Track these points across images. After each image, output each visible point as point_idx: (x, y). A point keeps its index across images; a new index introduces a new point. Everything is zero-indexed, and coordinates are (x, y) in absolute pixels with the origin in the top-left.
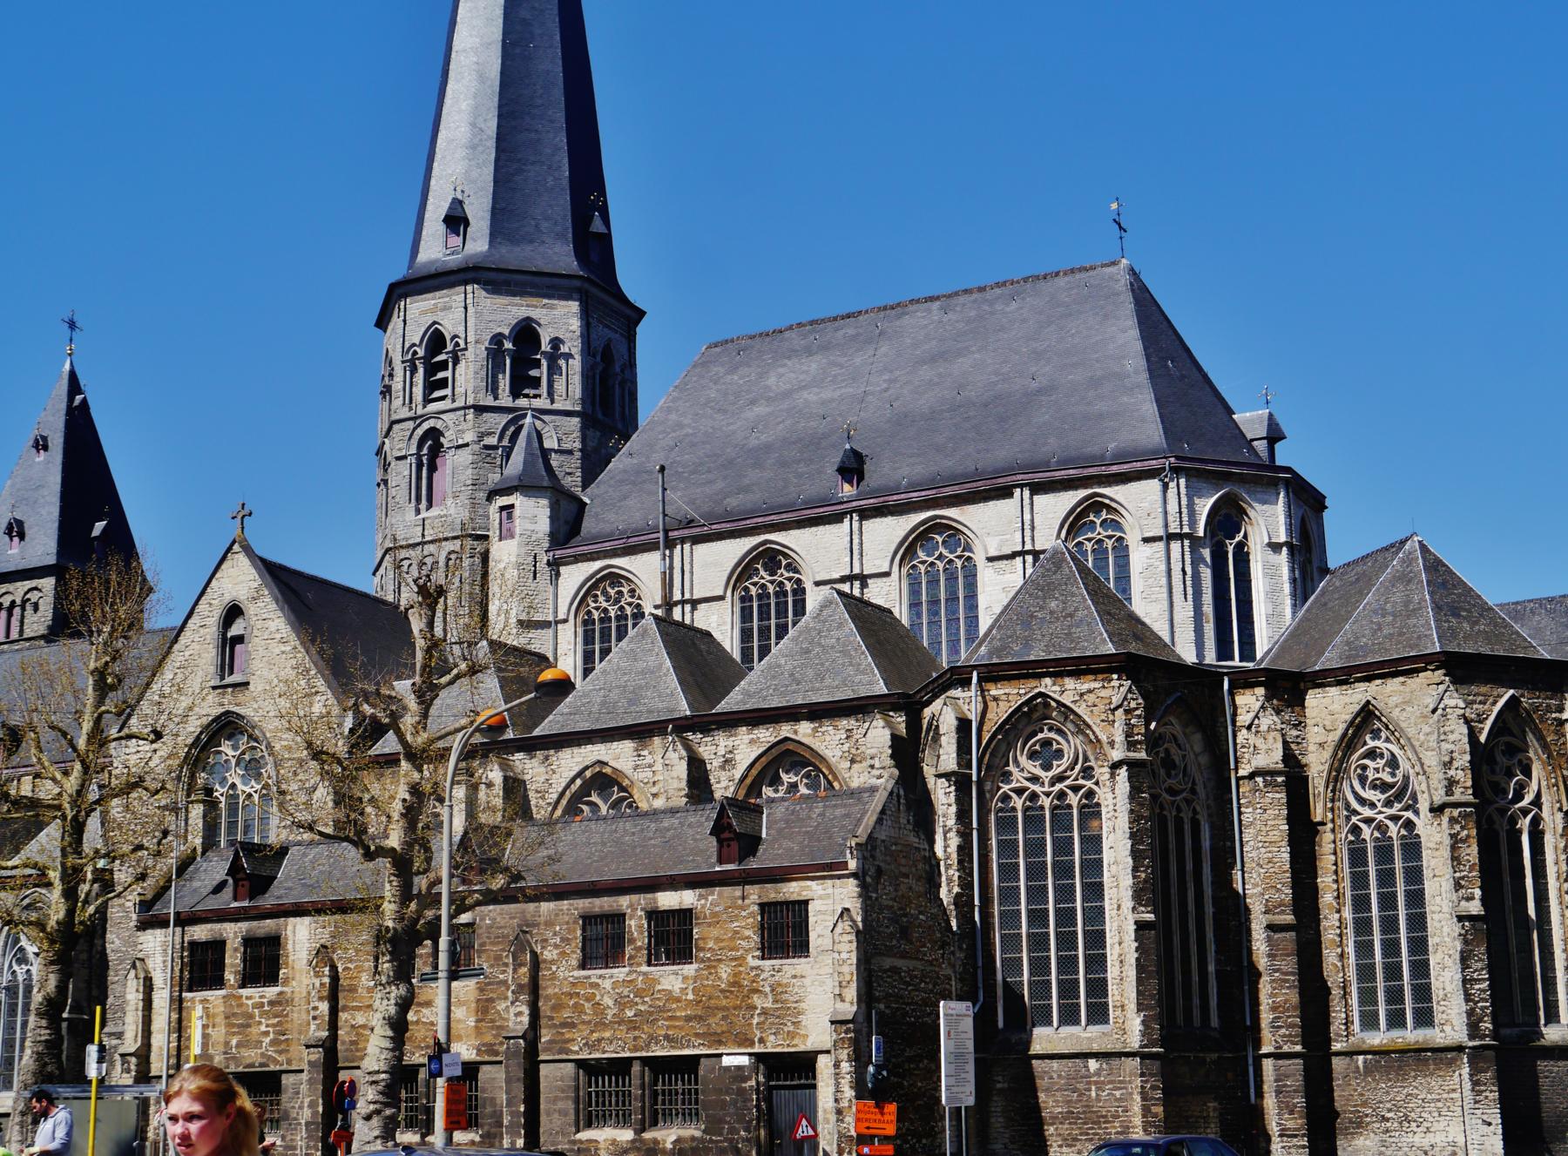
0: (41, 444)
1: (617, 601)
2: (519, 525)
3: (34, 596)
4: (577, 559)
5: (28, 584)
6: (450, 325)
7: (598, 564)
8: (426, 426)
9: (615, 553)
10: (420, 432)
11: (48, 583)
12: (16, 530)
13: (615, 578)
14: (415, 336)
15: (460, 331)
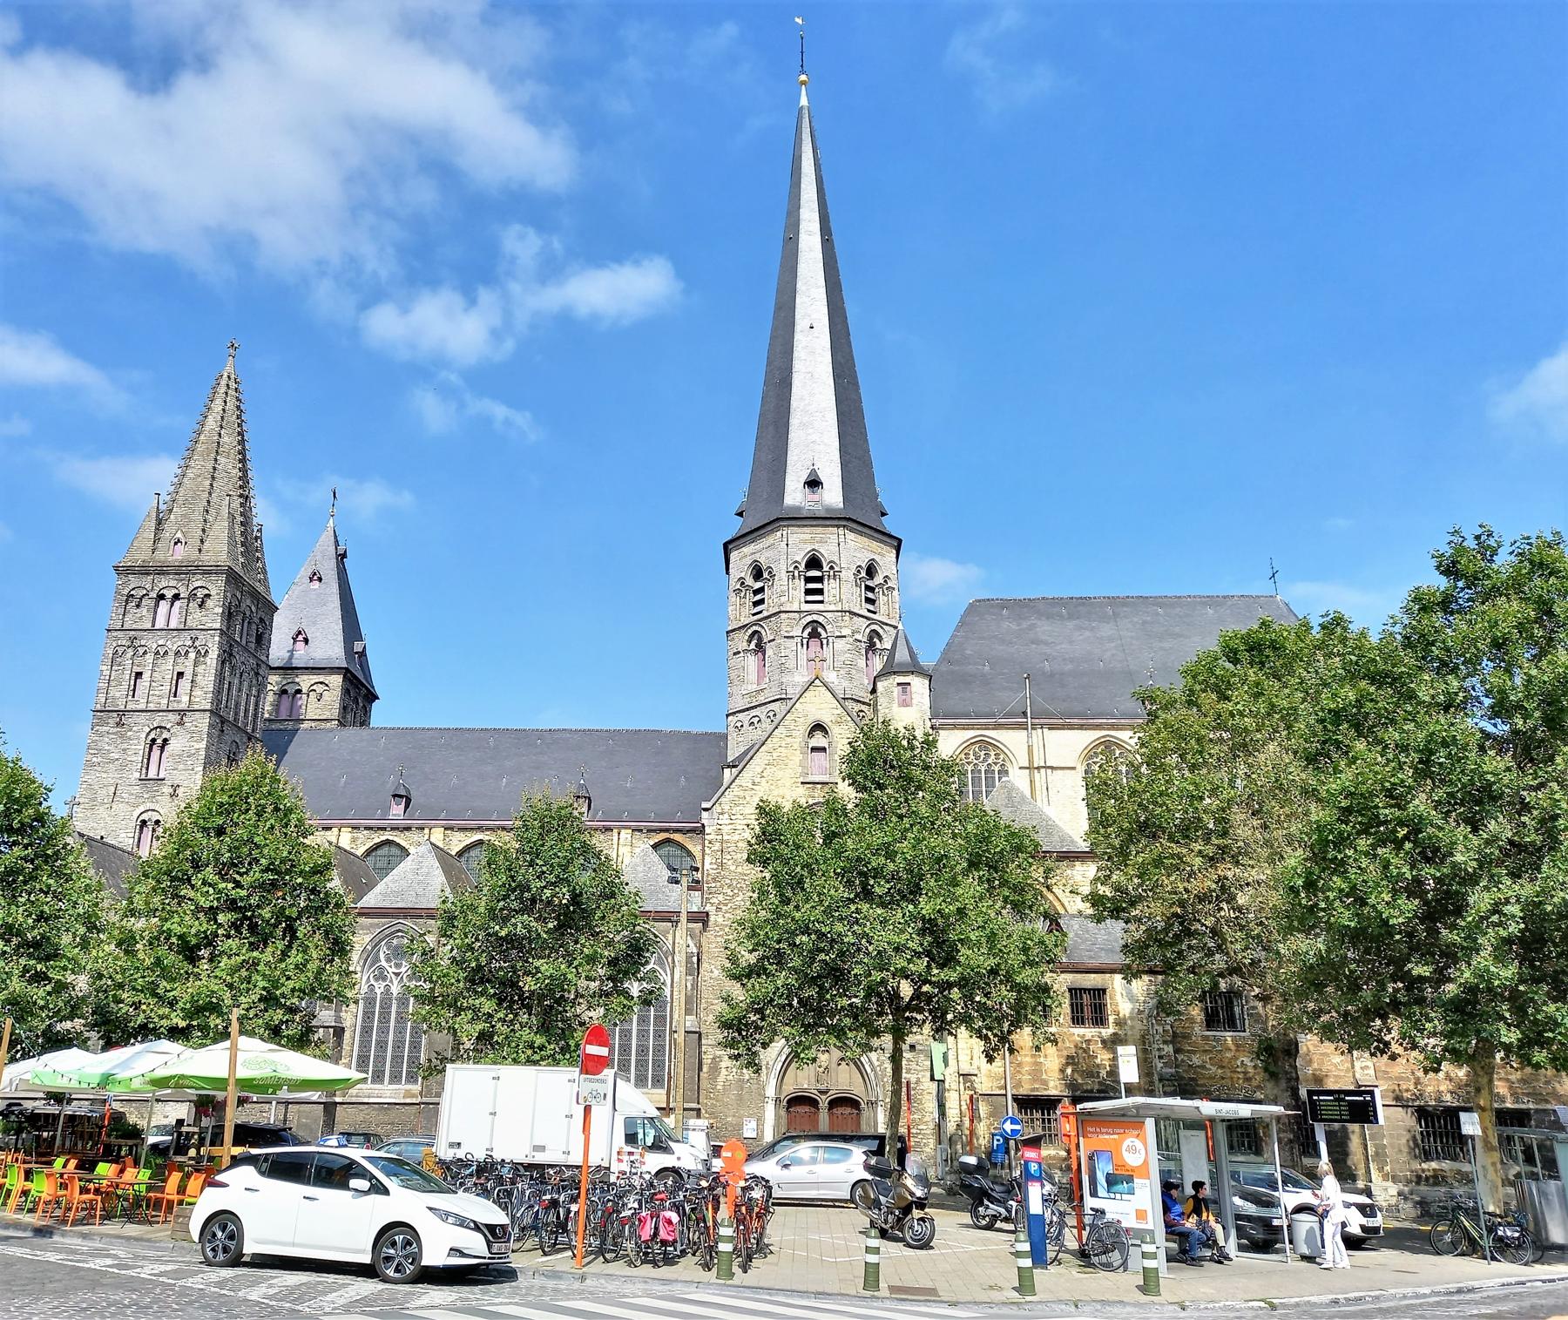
0: (316, 577)
1: (985, 760)
2: (916, 699)
3: (319, 688)
4: (955, 727)
5: (316, 678)
6: (827, 552)
7: (972, 733)
8: (809, 619)
9: (986, 727)
10: (805, 621)
11: (336, 680)
12: (300, 637)
13: (985, 744)
14: (801, 557)
15: (836, 559)
